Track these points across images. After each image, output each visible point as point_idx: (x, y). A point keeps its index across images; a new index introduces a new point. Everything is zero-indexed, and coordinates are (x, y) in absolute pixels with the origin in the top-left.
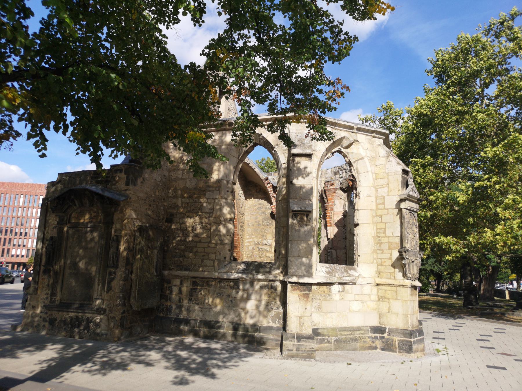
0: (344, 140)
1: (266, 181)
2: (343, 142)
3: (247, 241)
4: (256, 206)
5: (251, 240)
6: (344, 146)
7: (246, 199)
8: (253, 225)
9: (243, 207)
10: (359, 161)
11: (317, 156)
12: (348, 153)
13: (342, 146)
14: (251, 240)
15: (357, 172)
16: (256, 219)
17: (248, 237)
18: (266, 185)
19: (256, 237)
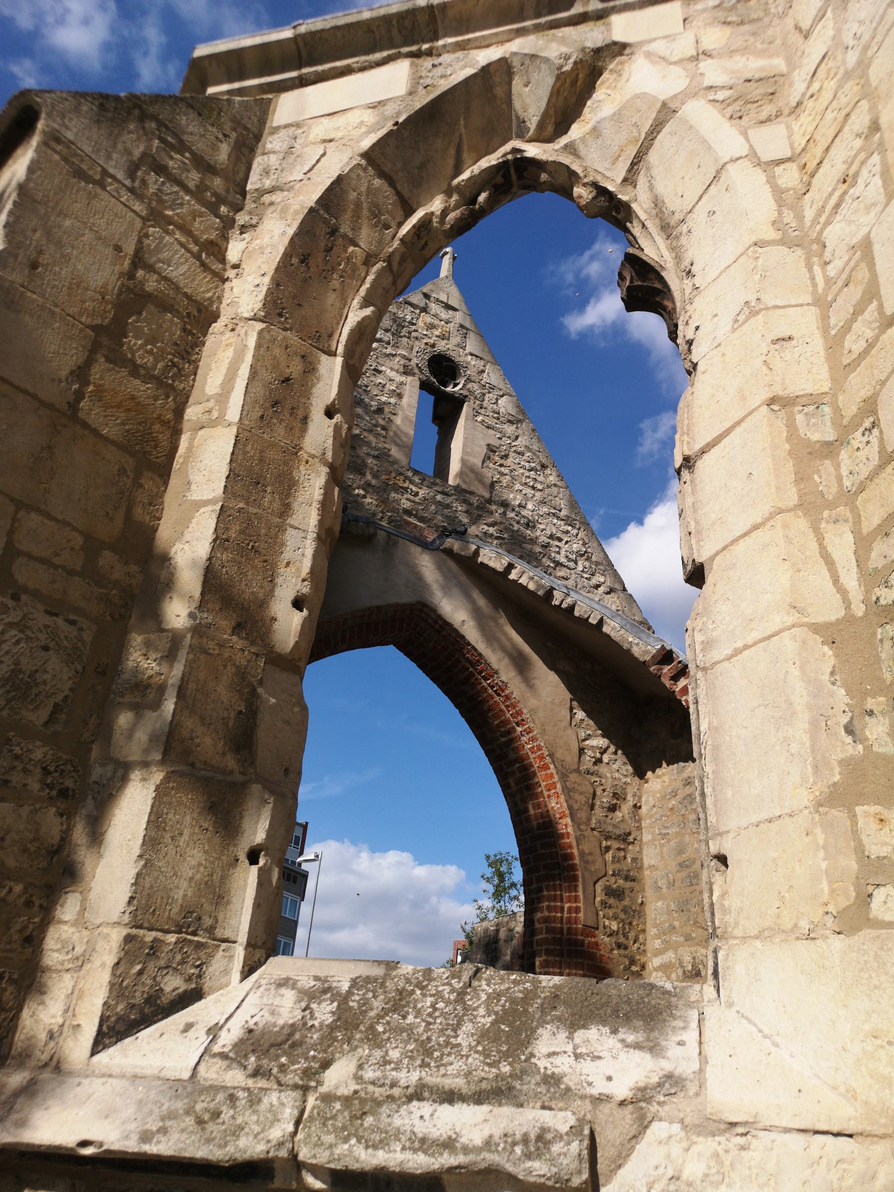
0: (517, 83)
1: (666, 669)
2: (517, 104)
3: (656, 962)
4: (674, 794)
5: (670, 956)
6: (532, 124)
7: (640, 773)
8: (671, 884)
9: (626, 808)
10: (653, 157)
11: (284, 210)
12: (570, 148)
13: (521, 136)
14: (670, 956)
15: (667, 229)
16: (680, 852)
17: (657, 944)
18: (667, 683)
19: (688, 938)
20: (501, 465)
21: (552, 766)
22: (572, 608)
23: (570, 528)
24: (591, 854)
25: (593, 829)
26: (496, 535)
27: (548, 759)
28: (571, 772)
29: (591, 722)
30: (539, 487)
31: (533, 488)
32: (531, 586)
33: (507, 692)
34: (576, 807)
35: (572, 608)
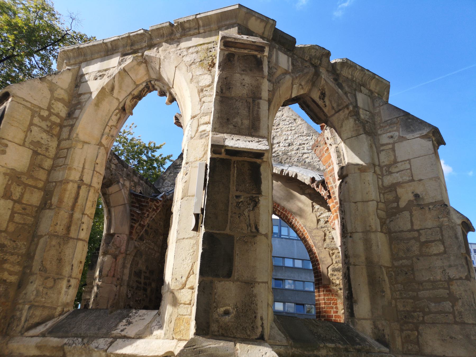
1: (315, 184)
20: (277, 129)
21: (305, 230)
22: (288, 174)
23: (308, 138)
24: (325, 257)
25: (325, 248)
26: (275, 155)
27: (304, 228)
28: (314, 230)
29: (322, 208)
30: (293, 128)
31: (291, 130)
32: (276, 172)
33: (285, 209)
34: (316, 242)
35: (288, 174)
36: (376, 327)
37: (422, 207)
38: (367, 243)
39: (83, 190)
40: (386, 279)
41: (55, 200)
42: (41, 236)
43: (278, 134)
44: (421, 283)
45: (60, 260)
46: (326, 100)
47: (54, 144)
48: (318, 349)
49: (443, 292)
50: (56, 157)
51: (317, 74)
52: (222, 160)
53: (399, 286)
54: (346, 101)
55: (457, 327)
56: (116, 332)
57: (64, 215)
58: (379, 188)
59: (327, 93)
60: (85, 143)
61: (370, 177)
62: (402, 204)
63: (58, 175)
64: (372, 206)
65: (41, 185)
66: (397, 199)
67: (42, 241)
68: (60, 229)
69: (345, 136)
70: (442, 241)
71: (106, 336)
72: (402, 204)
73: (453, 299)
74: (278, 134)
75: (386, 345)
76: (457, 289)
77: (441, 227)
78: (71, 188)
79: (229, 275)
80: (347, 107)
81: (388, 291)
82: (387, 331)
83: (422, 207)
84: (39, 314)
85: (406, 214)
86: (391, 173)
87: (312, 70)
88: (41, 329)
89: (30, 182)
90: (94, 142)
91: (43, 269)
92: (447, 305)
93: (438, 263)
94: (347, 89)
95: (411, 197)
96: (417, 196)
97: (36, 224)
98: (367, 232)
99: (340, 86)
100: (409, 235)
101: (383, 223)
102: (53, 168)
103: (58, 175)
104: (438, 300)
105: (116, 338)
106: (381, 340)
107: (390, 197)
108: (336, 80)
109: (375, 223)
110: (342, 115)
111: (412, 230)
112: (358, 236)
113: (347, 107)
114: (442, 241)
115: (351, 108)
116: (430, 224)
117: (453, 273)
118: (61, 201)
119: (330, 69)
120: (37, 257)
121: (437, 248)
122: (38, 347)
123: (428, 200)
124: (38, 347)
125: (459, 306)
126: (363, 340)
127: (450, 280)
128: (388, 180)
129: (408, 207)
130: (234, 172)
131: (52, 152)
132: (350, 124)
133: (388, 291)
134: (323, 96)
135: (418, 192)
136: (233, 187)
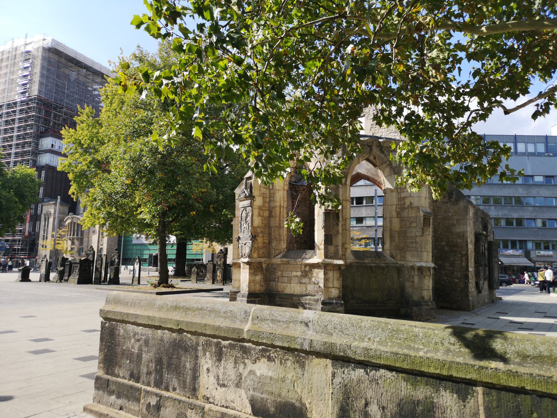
36: (391, 252)
37: (412, 208)
38: (391, 222)
39: (282, 209)
40: (397, 235)
41: (273, 214)
42: (272, 227)
43: (376, 131)
44: (408, 237)
45: (280, 235)
46: (377, 160)
47: (268, 192)
48: (365, 260)
49: (414, 240)
50: (270, 197)
51: (371, 150)
52: (328, 213)
53: (402, 238)
54: (385, 160)
55: (416, 252)
56: (303, 257)
57: (277, 219)
58: (398, 199)
59: (377, 157)
60: (279, 190)
61: (394, 194)
62: (406, 206)
63: (272, 204)
64: (394, 207)
65: (267, 209)
66: (405, 204)
67: (273, 229)
68: (277, 224)
69: (386, 175)
70: (416, 222)
71: (300, 258)
72: (406, 206)
73: (416, 243)
74: (376, 131)
75: (393, 258)
76: (418, 239)
77: (416, 216)
78: (278, 209)
79: (331, 244)
80: (386, 162)
81: (397, 240)
82: (394, 254)
83: (412, 208)
84: (277, 252)
85: (407, 210)
86: (404, 192)
87: (369, 149)
88: (279, 256)
89: (264, 209)
90: (282, 189)
91: (276, 238)
92: (414, 245)
93: (414, 230)
94: (386, 153)
95: (409, 204)
96: (411, 203)
97: (269, 223)
98: (391, 218)
99: (383, 153)
100: (406, 219)
101: (398, 213)
102: (270, 201)
103: (272, 204)
104: (412, 243)
105: (303, 259)
106: (392, 256)
107: (402, 202)
108: (380, 150)
109: (394, 214)
110: (384, 166)
111: (408, 217)
112: (388, 220)
113: (386, 162)
114: (416, 222)
115: (388, 163)
116: (413, 215)
117: (417, 234)
118: (275, 214)
119: (378, 145)
120: (272, 234)
121: (414, 225)
122: (281, 261)
123: (414, 205)
124: (281, 261)
125: (417, 246)
126: (384, 257)
127: (416, 236)
128: (403, 195)
129: (407, 208)
130: (331, 216)
131: (268, 195)
132: (388, 169)
133: (397, 240)
134: (375, 158)
135: (412, 201)
136: (331, 220)
